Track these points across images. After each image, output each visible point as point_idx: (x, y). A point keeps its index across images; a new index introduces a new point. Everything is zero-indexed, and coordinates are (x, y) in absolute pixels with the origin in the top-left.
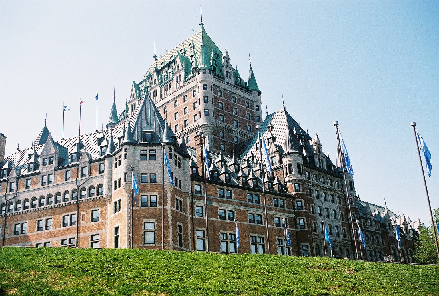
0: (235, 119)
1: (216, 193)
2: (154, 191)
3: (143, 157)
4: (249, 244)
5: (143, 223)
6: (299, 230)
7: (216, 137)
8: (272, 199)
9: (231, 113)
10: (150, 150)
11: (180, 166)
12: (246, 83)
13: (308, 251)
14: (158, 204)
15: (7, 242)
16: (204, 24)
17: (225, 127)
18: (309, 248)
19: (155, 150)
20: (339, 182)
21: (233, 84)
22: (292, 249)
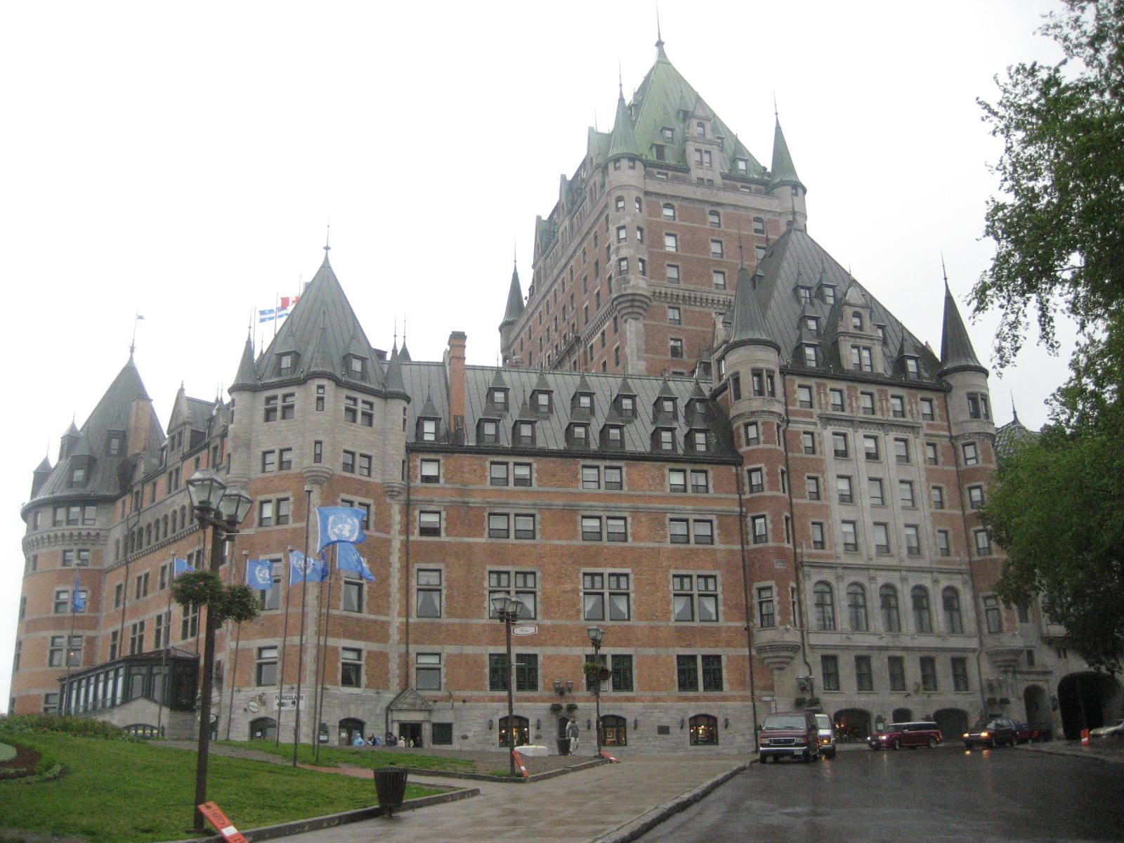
1: (483, 476)
2: (285, 491)
3: (269, 414)
6: (752, 546)
7: (656, 323)
8: (663, 475)
10: (285, 396)
11: (370, 424)
12: (765, 169)
13: (771, 601)
15: (127, 615)
17: (681, 294)
18: (775, 593)
19: (292, 395)
20: (935, 402)
21: (718, 181)
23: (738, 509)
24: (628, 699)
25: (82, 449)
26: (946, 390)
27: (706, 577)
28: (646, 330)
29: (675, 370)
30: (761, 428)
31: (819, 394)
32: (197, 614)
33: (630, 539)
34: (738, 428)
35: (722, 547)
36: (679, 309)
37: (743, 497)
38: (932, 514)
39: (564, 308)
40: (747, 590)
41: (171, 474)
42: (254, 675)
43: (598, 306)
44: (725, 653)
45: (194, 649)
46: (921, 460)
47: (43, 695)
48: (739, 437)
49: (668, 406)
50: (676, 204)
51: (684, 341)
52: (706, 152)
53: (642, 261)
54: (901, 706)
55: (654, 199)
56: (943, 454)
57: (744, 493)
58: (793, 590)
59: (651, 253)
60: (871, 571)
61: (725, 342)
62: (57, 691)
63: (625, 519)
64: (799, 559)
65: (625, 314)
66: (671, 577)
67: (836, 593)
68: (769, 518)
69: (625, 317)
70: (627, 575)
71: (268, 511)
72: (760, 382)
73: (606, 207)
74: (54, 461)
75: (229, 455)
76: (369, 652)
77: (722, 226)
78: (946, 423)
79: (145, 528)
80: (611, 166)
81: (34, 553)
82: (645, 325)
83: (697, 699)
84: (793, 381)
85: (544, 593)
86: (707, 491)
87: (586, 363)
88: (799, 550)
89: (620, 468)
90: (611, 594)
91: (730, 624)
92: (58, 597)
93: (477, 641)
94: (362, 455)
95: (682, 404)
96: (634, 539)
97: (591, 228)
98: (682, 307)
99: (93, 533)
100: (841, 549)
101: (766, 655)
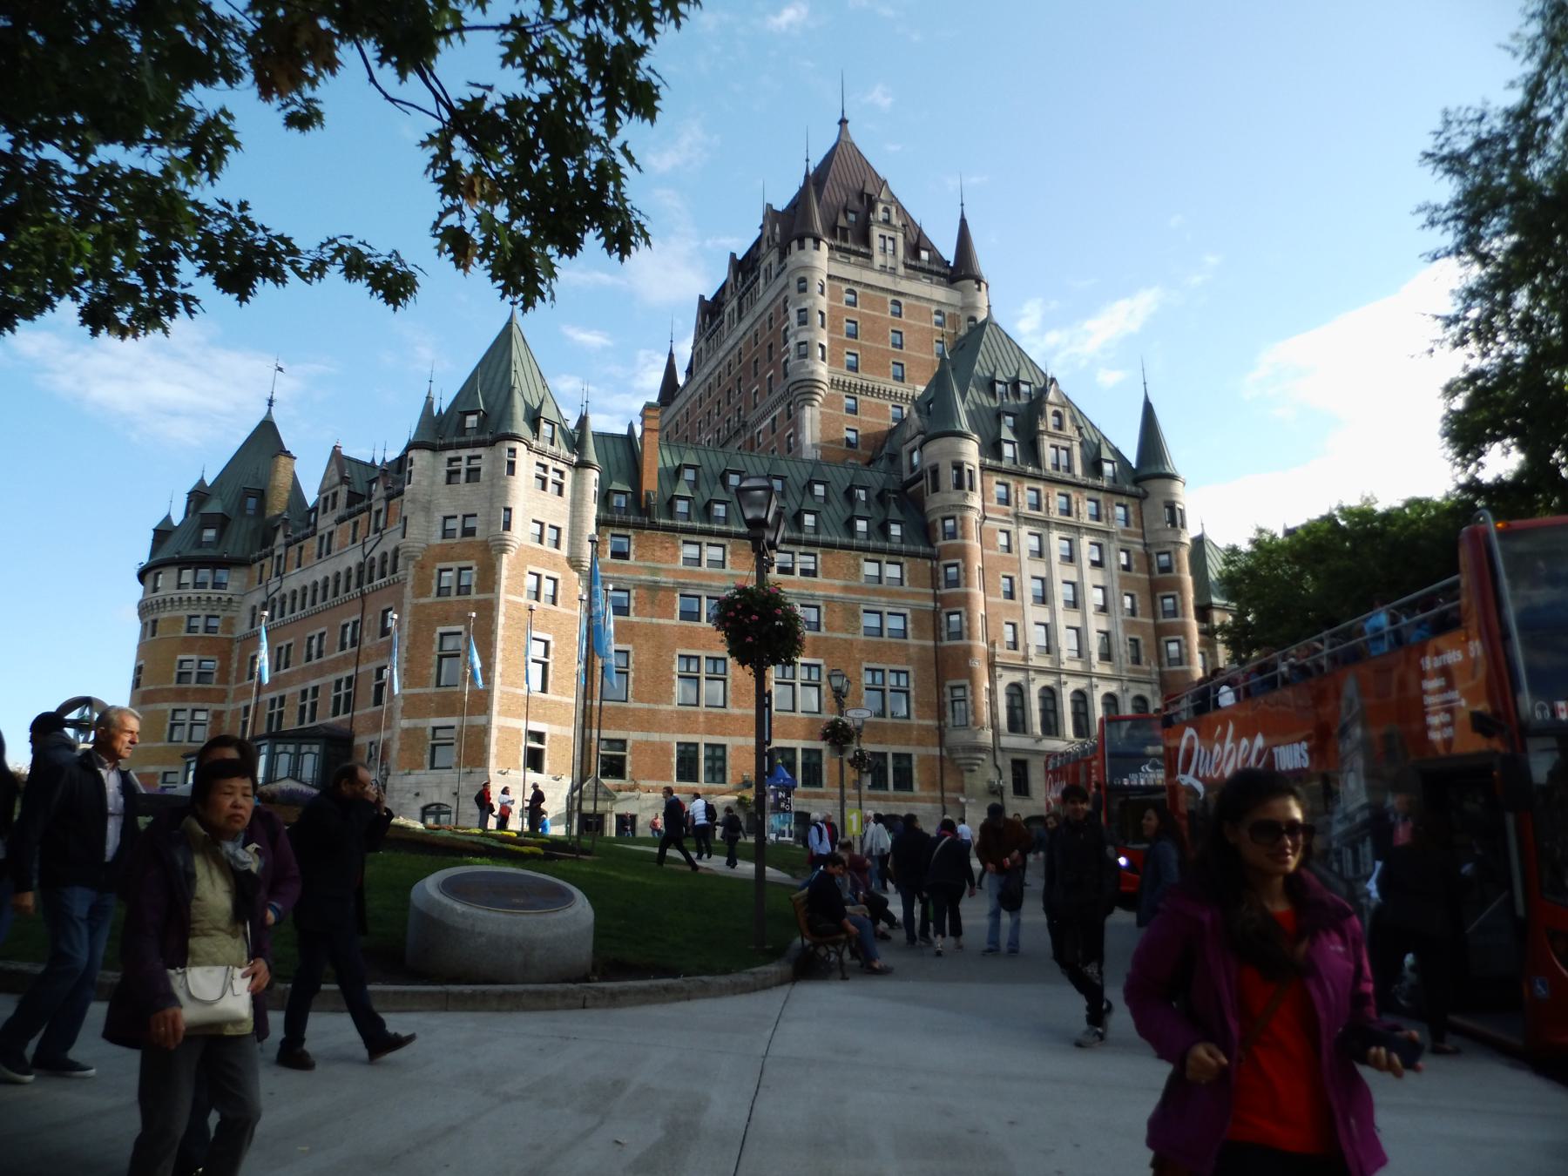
0: (896, 360)
1: (675, 557)
2: (467, 559)
3: (452, 476)
5: (437, 636)
6: (946, 643)
8: (858, 565)
10: (470, 458)
11: (560, 493)
14: (473, 590)
16: (847, 122)
19: (479, 457)
20: (1131, 509)
21: (901, 270)
22: (917, 696)
23: (932, 604)
24: (818, 796)
25: (214, 507)
26: (1142, 498)
27: (898, 672)
32: (351, 690)
33: (823, 629)
34: (936, 521)
36: (855, 399)
38: (1124, 622)
39: (729, 391)
40: (940, 685)
41: (322, 538)
42: (427, 757)
44: (916, 752)
45: (348, 727)
46: (1114, 565)
47: (161, 773)
48: (936, 530)
50: (858, 289)
55: (836, 283)
56: (1137, 562)
59: (831, 340)
61: (920, 433)
62: (181, 770)
63: (818, 607)
70: (818, 666)
71: (448, 578)
73: (786, 286)
74: (177, 519)
75: (405, 519)
76: (552, 736)
78: (1140, 531)
79: (299, 590)
80: (795, 244)
81: (153, 617)
82: (821, 413)
83: (886, 799)
85: (734, 680)
86: (902, 584)
89: (815, 555)
90: (802, 685)
91: (921, 722)
92: (180, 667)
93: (667, 730)
94: (551, 526)
95: (874, 493)
96: (828, 629)
97: (766, 310)
99: (225, 598)
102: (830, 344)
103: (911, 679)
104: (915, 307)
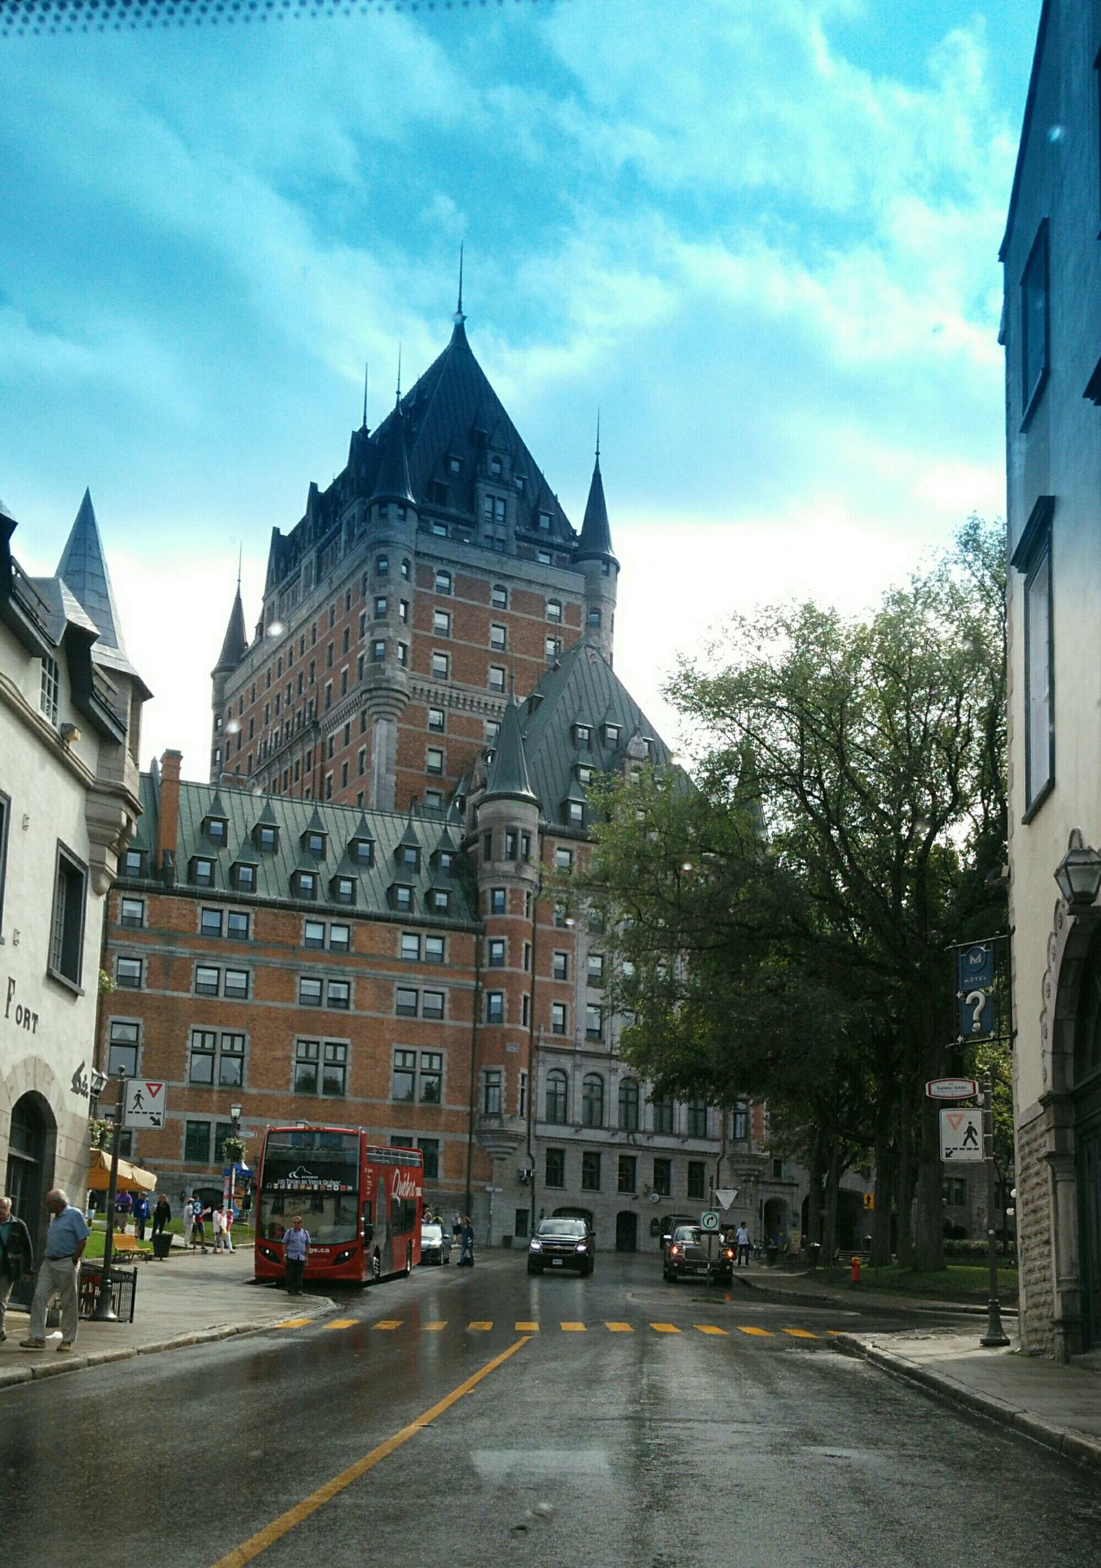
0: (496, 664)
4: (289, 1063)
7: (412, 728)
9: (478, 646)
17: (447, 693)
18: (503, 1079)
22: (449, 1079)
23: (474, 983)
27: (431, 1055)
28: (400, 737)
29: (430, 789)
30: (509, 896)
31: (580, 859)
33: (352, 1006)
34: (485, 892)
35: (452, 1023)
37: (481, 970)
39: (301, 676)
40: (474, 1070)
43: (344, 691)
48: (485, 902)
49: (410, 855)
51: (445, 754)
52: (500, 499)
53: (404, 646)
54: (627, 1208)
57: (482, 966)
58: (523, 1076)
59: (415, 637)
60: (613, 1062)
63: (348, 983)
64: (535, 1042)
65: (375, 713)
66: (392, 1052)
67: (570, 1082)
68: (506, 995)
69: (375, 717)
70: (345, 1046)
72: (514, 844)
77: (509, 607)
82: (399, 730)
84: (552, 843)
85: (252, 1059)
87: (323, 760)
88: (535, 1034)
90: (325, 1065)
91: (451, 1107)
96: (357, 1007)
98: (445, 709)
100: (582, 1035)
101: (487, 1144)
102: (413, 642)
103: (444, 1063)
104: (524, 594)
